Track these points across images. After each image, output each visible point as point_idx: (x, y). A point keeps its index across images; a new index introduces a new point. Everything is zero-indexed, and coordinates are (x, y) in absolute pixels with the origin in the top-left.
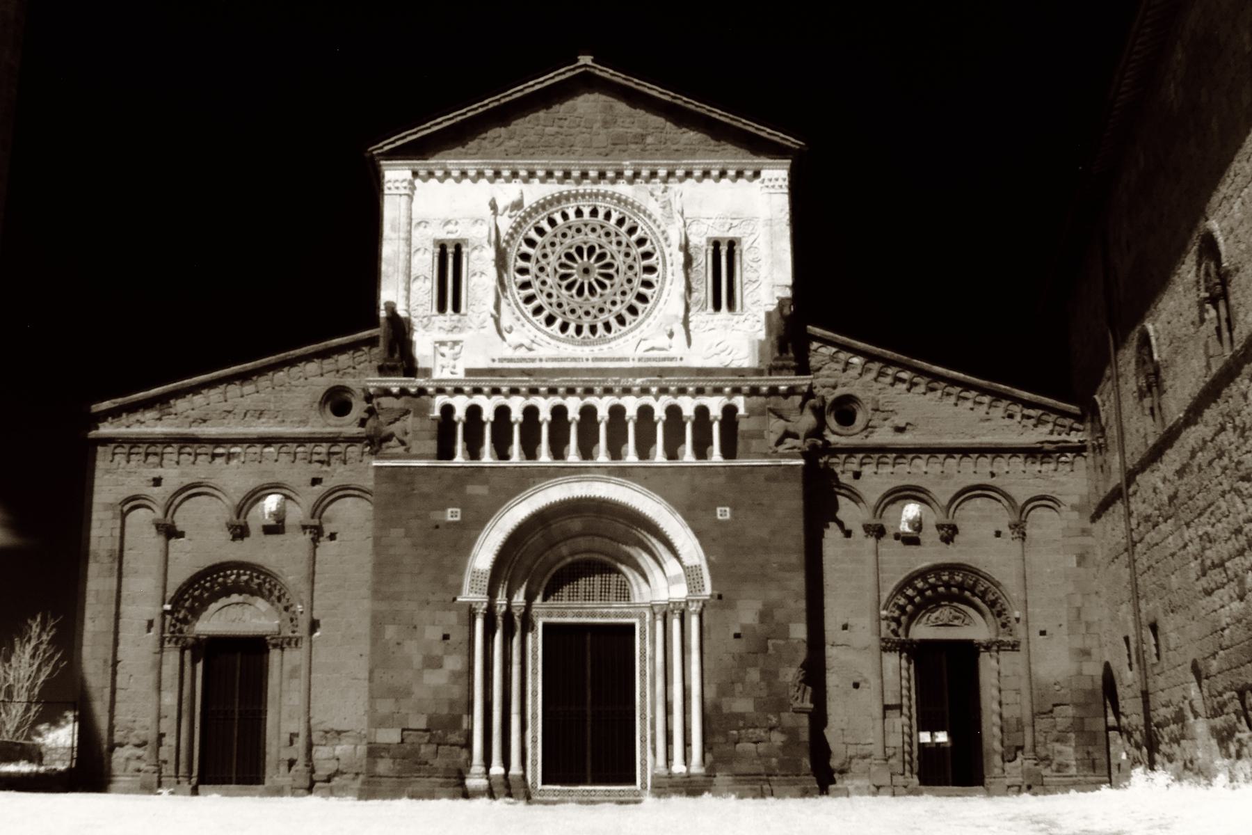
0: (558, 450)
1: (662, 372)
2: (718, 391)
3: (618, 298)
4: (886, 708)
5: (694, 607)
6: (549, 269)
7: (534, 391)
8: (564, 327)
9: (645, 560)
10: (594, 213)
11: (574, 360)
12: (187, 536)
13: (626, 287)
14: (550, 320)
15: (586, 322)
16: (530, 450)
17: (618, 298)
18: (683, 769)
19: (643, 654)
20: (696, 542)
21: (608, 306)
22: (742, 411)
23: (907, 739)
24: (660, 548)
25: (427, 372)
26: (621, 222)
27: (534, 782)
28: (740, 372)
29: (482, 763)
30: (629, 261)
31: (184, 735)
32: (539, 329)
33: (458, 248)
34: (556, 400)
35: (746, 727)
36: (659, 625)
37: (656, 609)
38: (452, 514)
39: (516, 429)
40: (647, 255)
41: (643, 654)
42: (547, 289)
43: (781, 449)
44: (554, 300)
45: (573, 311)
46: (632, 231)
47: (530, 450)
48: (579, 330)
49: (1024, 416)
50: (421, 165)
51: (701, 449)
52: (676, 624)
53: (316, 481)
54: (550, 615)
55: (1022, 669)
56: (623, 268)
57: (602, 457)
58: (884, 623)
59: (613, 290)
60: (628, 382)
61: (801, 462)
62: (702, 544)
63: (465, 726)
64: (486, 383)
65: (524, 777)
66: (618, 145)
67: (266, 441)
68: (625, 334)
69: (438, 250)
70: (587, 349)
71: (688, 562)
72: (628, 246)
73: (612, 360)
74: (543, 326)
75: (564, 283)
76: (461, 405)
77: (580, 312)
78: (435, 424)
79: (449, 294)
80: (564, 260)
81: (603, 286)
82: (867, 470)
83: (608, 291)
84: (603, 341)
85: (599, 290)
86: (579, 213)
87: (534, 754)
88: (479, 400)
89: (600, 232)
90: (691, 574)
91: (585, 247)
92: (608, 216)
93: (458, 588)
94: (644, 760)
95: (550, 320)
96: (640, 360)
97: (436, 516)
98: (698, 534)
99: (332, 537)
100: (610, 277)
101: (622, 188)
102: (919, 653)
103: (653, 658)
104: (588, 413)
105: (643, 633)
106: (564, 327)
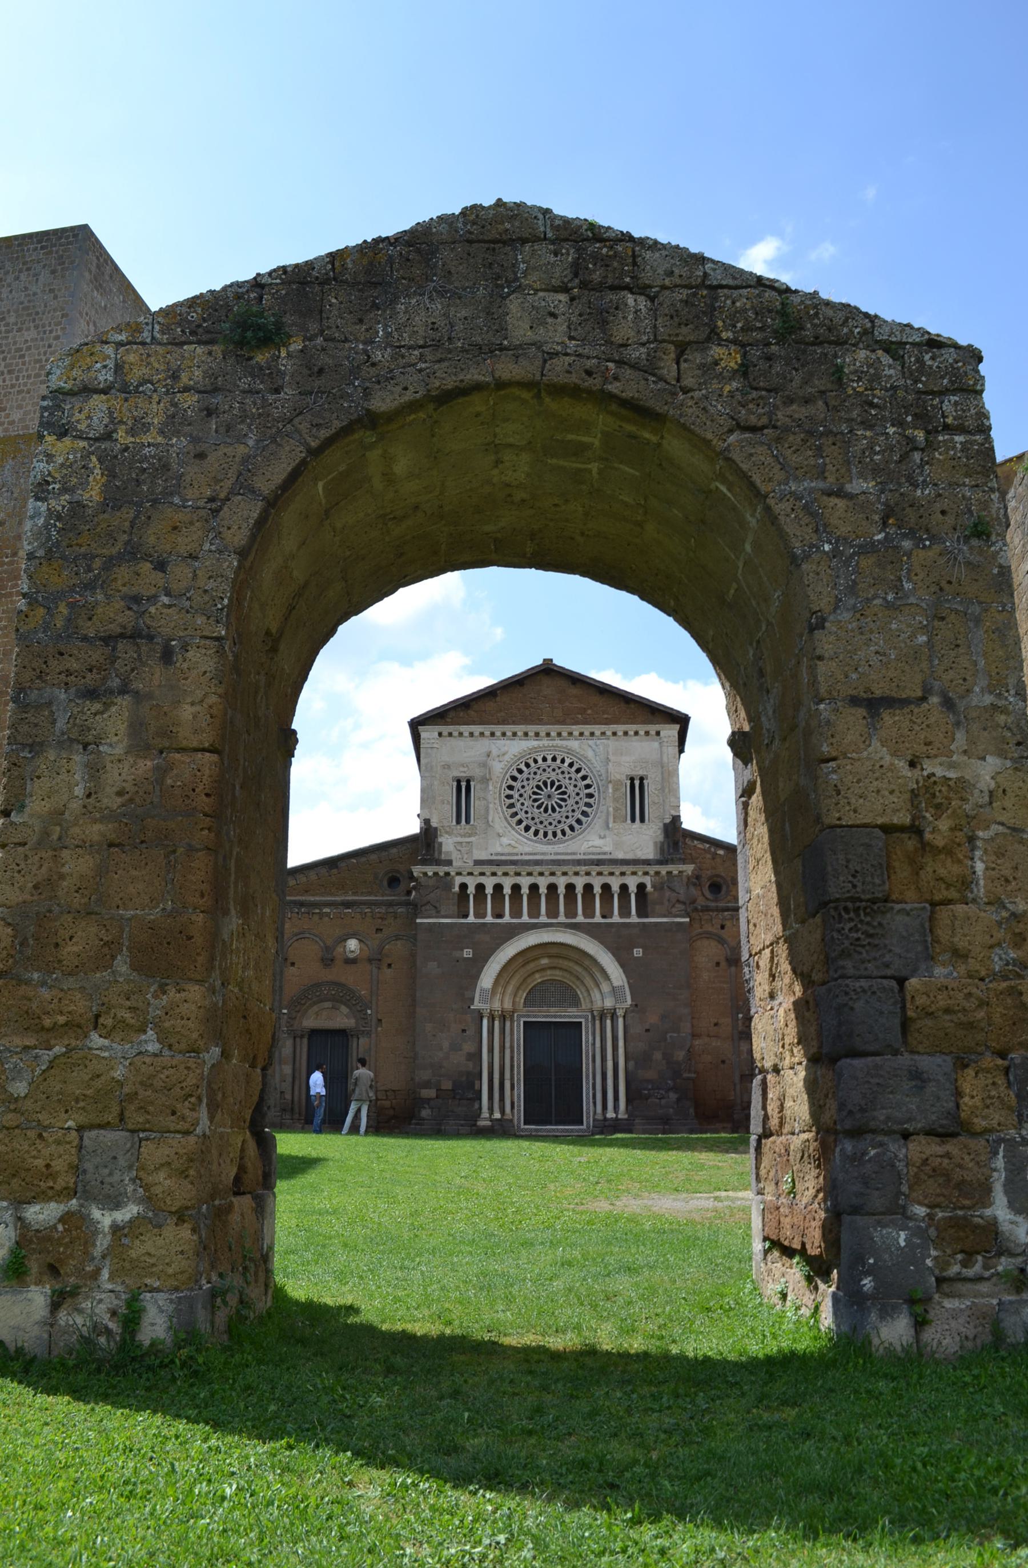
0: (534, 912)
1: (599, 863)
2: (634, 873)
3: (570, 814)
7: (518, 874)
8: (536, 833)
9: (588, 981)
10: (554, 759)
13: (575, 807)
14: (527, 829)
16: (516, 913)
17: (570, 814)
19: (587, 1042)
21: (563, 819)
22: (649, 888)
24: (598, 975)
25: (449, 863)
26: (571, 765)
28: (647, 862)
30: (577, 790)
31: (296, 1093)
33: (468, 782)
36: (597, 1023)
38: (468, 953)
39: (507, 898)
40: (588, 786)
41: (587, 1042)
42: (525, 808)
43: (674, 910)
46: (578, 771)
47: (516, 913)
48: (545, 834)
50: (445, 729)
51: (625, 911)
52: (609, 1022)
53: (379, 930)
54: (529, 1016)
57: (562, 919)
64: (488, 869)
65: (511, 1121)
66: (567, 718)
67: (347, 905)
71: (616, 984)
76: (471, 883)
77: (546, 823)
81: (560, 806)
86: (545, 759)
88: (482, 880)
92: (563, 761)
94: (588, 1109)
95: (527, 829)
97: (457, 954)
98: (622, 966)
99: (389, 966)
100: (564, 800)
101: (574, 744)
103: (594, 1044)
104: (552, 888)
105: (587, 1028)
106: (536, 833)
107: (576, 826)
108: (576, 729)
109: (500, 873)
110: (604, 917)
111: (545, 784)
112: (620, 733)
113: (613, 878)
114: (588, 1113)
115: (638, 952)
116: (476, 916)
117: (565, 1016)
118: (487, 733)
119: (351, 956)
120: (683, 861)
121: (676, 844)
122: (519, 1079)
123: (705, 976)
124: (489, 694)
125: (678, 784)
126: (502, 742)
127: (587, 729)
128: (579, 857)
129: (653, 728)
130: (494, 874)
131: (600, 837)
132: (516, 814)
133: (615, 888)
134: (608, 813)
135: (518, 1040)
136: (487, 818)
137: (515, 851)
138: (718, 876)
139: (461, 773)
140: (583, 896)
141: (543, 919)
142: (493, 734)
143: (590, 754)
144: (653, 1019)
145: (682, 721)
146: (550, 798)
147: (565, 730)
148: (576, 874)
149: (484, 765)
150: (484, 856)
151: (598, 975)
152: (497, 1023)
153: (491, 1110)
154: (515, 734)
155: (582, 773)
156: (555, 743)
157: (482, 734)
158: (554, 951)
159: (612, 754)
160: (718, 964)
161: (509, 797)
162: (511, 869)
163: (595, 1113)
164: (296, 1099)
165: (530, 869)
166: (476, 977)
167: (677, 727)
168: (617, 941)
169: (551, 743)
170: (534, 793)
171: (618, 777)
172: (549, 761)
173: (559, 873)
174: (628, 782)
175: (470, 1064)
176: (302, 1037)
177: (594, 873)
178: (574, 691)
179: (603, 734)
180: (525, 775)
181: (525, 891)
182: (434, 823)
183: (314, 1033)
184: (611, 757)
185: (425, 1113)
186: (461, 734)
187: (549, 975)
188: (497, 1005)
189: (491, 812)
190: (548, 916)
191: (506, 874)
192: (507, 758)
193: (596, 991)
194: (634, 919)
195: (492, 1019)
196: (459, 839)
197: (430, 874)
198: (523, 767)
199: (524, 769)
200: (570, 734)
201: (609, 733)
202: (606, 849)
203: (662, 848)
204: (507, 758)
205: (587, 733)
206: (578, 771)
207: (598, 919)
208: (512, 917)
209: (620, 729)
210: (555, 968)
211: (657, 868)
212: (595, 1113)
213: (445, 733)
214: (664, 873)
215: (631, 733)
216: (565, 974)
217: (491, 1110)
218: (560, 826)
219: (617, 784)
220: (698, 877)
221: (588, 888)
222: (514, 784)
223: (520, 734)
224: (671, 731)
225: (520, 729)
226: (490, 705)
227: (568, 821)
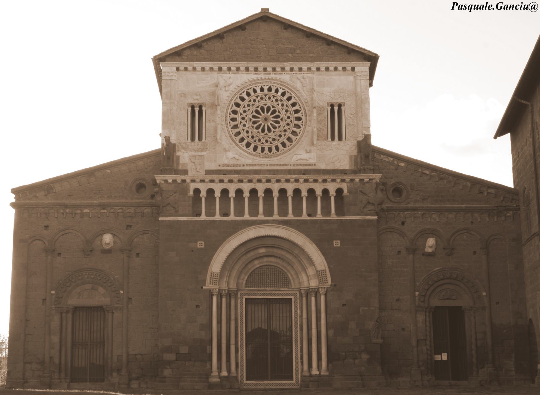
0: (254, 211)
1: (305, 172)
2: (333, 180)
3: (282, 134)
4: (418, 341)
5: (322, 291)
6: (246, 118)
7: (241, 181)
8: (255, 149)
10: (270, 89)
11: (260, 165)
12: (62, 256)
14: (248, 145)
15: (266, 146)
16: (240, 212)
18: (318, 373)
20: (323, 258)
21: (277, 138)
22: (345, 192)
23: (429, 357)
24: (305, 262)
25: (185, 172)
26: (283, 94)
27: (242, 378)
28: (344, 172)
29: (216, 370)
30: (288, 114)
32: (243, 150)
33: (201, 107)
34: (251, 186)
36: (304, 299)
37: (303, 292)
38: (200, 245)
39: (232, 200)
40: (297, 111)
42: (246, 129)
44: (250, 134)
45: (259, 140)
46: (289, 99)
47: (240, 212)
48: (263, 150)
49: (488, 193)
50: (182, 65)
52: (313, 299)
54: (250, 294)
56: (285, 118)
58: (417, 298)
59: (280, 129)
60: (289, 177)
61: (376, 217)
62: (326, 259)
63: (208, 352)
64: (216, 177)
65: (236, 378)
66: (281, 55)
68: (286, 152)
69: (190, 109)
70: (266, 159)
72: (287, 106)
73: (280, 165)
74: (245, 148)
75: (255, 126)
76: (203, 188)
77: (263, 141)
79: (196, 131)
80: (255, 114)
81: (275, 128)
83: (277, 129)
85: (273, 129)
86: (262, 90)
87: (242, 366)
89: (272, 99)
90: (319, 274)
91: (265, 107)
92: (277, 91)
93: (205, 281)
95: (248, 145)
96: (294, 165)
98: (324, 254)
100: (278, 122)
101: (285, 77)
102: (436, 313)
103: (301, 316)
104: (268, 192)
105: (296, 303)
106: (255, 149)
108: (288, 66)
109: (226, 180)
110: (309, 215)
111: (262, 109)
112: (323, 69)
114: (297, 371)
115: (337, 243)
116: (207, 215)
117: (278, 294)
118: (216, 68)
119: (107, 247)
120: (374, 171)
121: (367, 157)
122: (242, 345)
124: (219, 36)
125: (368, 109)
126: (227, 76)
127: (296, 65)
128: (289, 168)
129: (349, 65)
130: (221, 181)
131: (307, 152)
133: (319, 192)
134: (313, 132)
135: (241, 313)
136: (215, 136)
137: (239, 163)
140: (293, 198)
141: (261, 217)
142: (220, 69)
143: (298, 85)
145: (372, 59)
147: (278, 66)
148: (288, 181)
149: (213, 94)
150: (213, 167)
151: (305, 262)
152: (224, 300)
153: (220, 369)
154: (238, 69)
156: (270, 76)
157: (212, 69)
158: (270, 242)
159: (315, 85)
160: (399, 252)
161: (233, 120)
162: (235, 177)
164: (63, 362)
165: (250, 177)
166: (207, 264)
167: (369, 64)
168: (321, 235)
169: (267, 76)
170: (254, 117)
171: (321, 104)
172: (266, 91)
173: (273, 180)
174: (329, 108)
176: (67, 312)
178: (287, 34)
179: (309, 69)
180: (246, 102)
181: (246, 194)
182: (173, 140)
183: (77, 309)
184: (315, 88)
185: (167, 372)
186: (194, 69)
188: (224, 286)
189: (219, 132)
191: (231, 181)
192: (232, 88)
194: (333, 217)
195: (220, 296)
196: (193, 153)
197: (170, 181)
199: (246, 97)
200: (283, 69)
201: (314, 69)
202: (312, 161)
203: (354, 160)
205: (296, 69)
206: (289, 99)
208: (236, 215)
209: (323, 65)
210: (271, 256)
211: (352, 176)
213: (182, 68)
214: (357, 180)
215: (332, 69)
216: (279, 261)
217: (220, 369)
218: (275, 143)
219: (320, 110)
220: (384, 184)
221: (297, 192)
222: (237, 109)
223: (242, 69)
225: (242, 65)
226: (218, 45)
227: (281, 139)
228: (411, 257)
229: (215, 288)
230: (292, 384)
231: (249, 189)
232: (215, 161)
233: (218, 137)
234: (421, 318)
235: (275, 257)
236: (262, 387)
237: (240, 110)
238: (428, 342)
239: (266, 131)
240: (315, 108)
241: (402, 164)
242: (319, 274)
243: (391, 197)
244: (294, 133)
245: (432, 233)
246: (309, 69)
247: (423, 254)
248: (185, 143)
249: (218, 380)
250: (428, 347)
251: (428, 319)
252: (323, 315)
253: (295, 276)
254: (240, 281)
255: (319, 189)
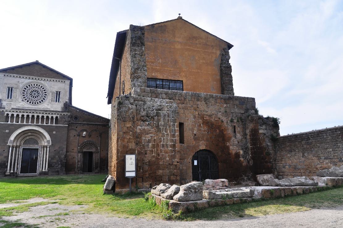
0: (27, 121)
1: (46, 111)
2: (55, 114)
3: (40, 99)
8: (30, 103)
9: (41, 139)
10: (37, 85)
14: (28, 101)
18: (44, 171)
22: (59, 118)
25: (4, 108)
26: (41, 87)
33: (12, 88)
35: (55, 164)
38: (7, 131)
40: (45, 92)
41: (39, 153)
43: (64, 123)
46: (43, 88)
48: (33, 103)
50: (6, 74)
51: (52, 122)
52: (45, 149)
55: (99, 156)
57: (35, 123)
60: (40, 112)
71: (48, 139)
76: (10, 114)
78: (5, 118)
80: (31, 92)
82: (78, 127)
84: (36, 105)
86: (34, 85)
90: (48, 142)
92: (39, 86)
93: (7, 143)
95: (28, 101)
97: (4, 131)
100: (39, 95)
101: (42, 82)
102: (84, 154)
103: (41, 154)
106: (30, 103)
107: (41, 102)
108: (43, 78)
109: (18, 112)
110: (46, 124)
113: (50, 115)
115: (54, 132)
118: (18, 77)
120: (68, 112)
122: (20, 162)
123: (71, 138)
127: (46, 79)
129: (63, 81)
130: (17, 112)
132: (25, 97)
133: (50, 117)
137: (24, 106)
138: (77, 116)
139: (10, 86)
141: (30, 123)
143: (47, 85)
144: (57, 148)
146: (34, 95)
148: (40, 113)
150: (15, 107)
152: (14, 148)
155: (44, 89)
157: (17, 77)
159: (52, 86)
160: (75, 136)
163: (40, 170)
168: (49, 130)
174: (56, 93)
175: (5, 159)
177: (44, 113)
178: (43, 69)
187: (31, 137)
188: (15, 144)
190: (31, 123)
191: (20, 112)
193: (43, 141)
194: (54, 125)
195: (13, 147)
196: (8, 103)
198: (28, 86)
199: (28, 87)
202: (48, 108)
204: (23, 83)
205: (46, 80)
206: (43, 88)
207: (45, 124)
212: (40, 170)
213: (6, 75)
216: (34, 137)
219: (53, 93)
220: (72, 116)
221: (43, 117)
224: (68, 82)
225: (28, 77)
226: (20, 70)
228: (78, 137)
229: (11, 145)
230: (36, 174)
231: (27, 115)
232: (16, 105)
233: (17, 98)
234: (79, 155)
235: (34, 136)
236: (26, 175)
237: (26, 90)
238: (81, 161)
239: (34, 98)
240: (51, 92)
241: (78, 111)
242: (48, 142)
243: (74, 120)
244: (44, 99)
245: (85, 130)
246: (50, 80)
247: (82, 136)
248: (5, 99)
249: (9, 174)
250: (81, 163)
251: (82, 155)
252: (48, 153)
253: (40, 142)
254: (21, 143)
255: (50, 116)
